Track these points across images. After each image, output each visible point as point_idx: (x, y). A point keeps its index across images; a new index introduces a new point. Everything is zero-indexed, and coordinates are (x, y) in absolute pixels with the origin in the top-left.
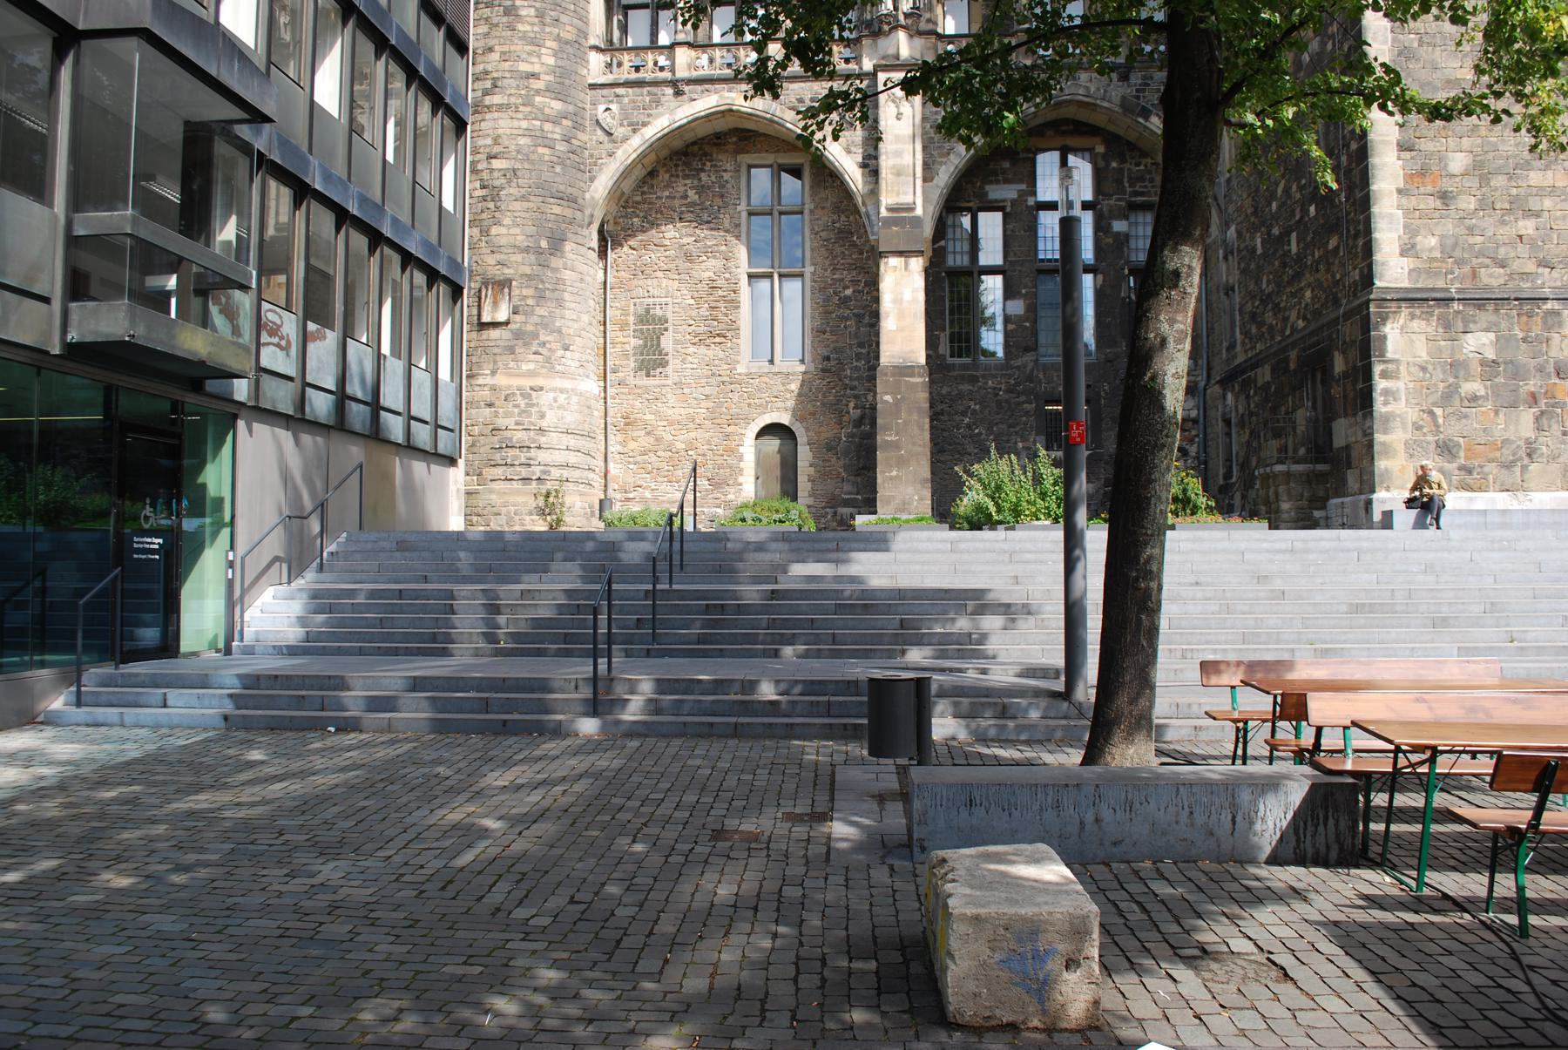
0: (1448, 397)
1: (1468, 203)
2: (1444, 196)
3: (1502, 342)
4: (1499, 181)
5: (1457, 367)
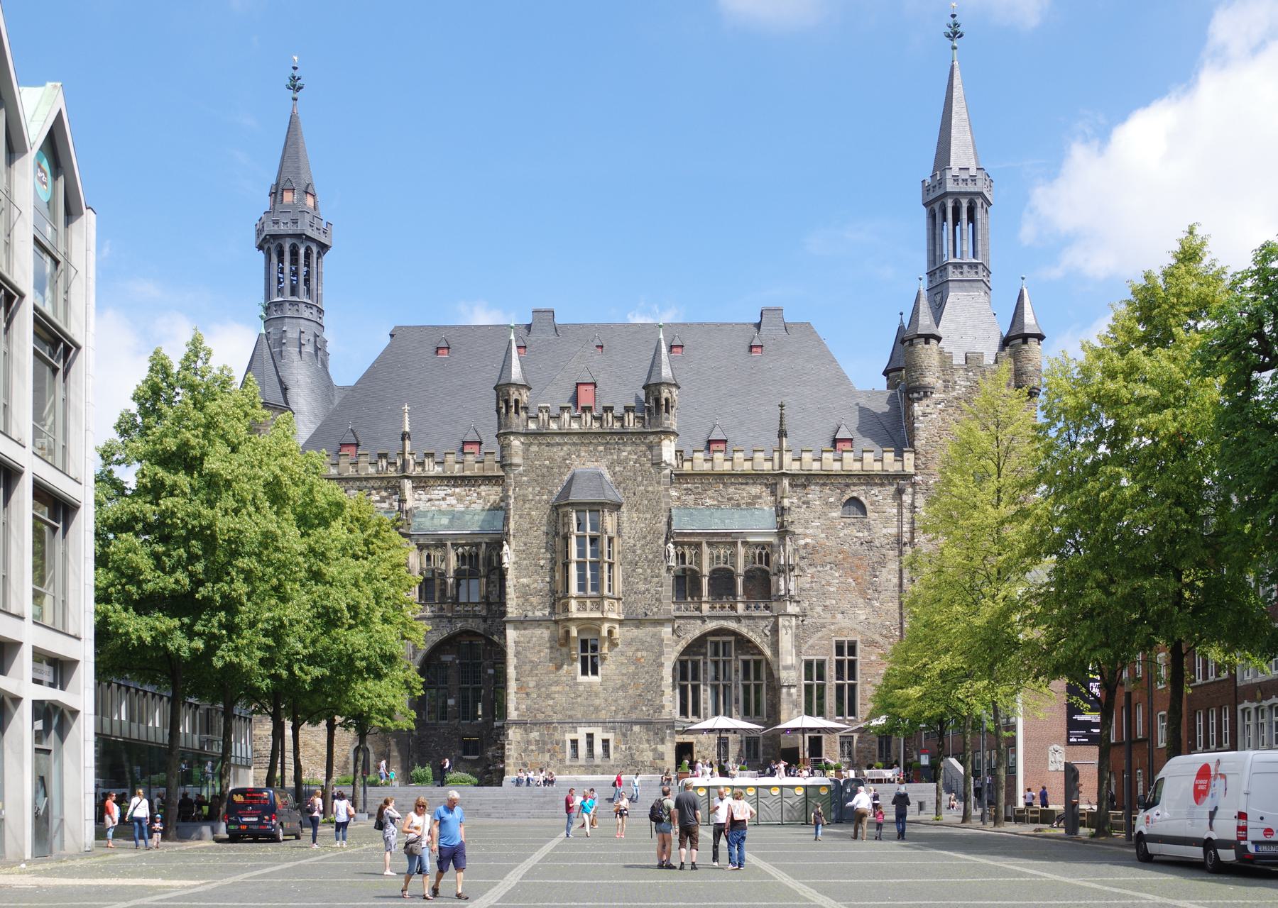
0: (525, 751)
2: (527, 694)
3: (542, 735)
5: (529, 742)
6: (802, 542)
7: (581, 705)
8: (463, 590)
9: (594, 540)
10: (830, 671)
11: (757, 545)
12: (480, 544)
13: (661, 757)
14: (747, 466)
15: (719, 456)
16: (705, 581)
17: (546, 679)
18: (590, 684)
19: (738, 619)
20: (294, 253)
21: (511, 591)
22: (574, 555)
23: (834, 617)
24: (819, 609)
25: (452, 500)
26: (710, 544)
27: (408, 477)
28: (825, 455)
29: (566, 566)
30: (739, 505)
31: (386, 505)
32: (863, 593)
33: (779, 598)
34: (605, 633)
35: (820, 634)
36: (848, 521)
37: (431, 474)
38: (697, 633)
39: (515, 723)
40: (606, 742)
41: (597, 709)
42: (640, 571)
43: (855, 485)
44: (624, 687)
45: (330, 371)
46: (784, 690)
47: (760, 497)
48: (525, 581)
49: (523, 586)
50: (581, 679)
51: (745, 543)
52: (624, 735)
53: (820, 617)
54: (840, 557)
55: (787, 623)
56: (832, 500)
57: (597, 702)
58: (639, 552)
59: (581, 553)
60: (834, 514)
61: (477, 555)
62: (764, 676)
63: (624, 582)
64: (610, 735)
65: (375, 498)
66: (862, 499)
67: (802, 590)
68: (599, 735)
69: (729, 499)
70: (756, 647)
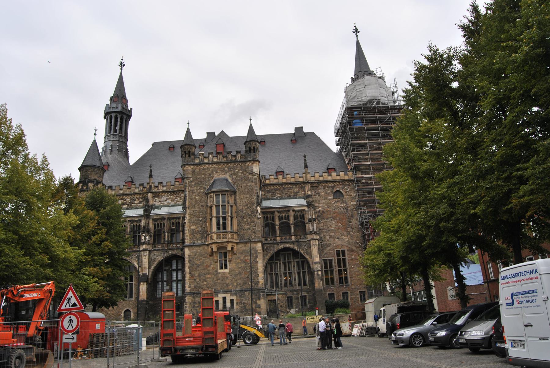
1: (198, 280)
4: (202, 277)
5: (195, 303)
6: (318, 210)
7: (220, 283)
8: (174, 238)
9: (224, 206)
10: (335, 264)
11: (299, 211)
12: (179, 218)
13: (259, 306)
14: (293, 180)
15: (280, 177)
16: (277, 228)
17: (203, 272)
18: (224, 273)
19: (293, 243)
20: (116, 118)
21: (187, 232)
22: (214, 214)
23: (334, 240)
24: (328, 237)
25: (169, 201)
26: (277, 211)
27: (151, 192)
28: (324, 174)
29: (211, 219)
30: (290, 196)
31: (141, 205)
32: (345, 229)
33: (311, 233)
34: (229, 248)
35: (329, 248)
36: (336, 200)
37: (161, 190)
38: (275, 250)
39: (190, 294)
40: (232, 301)
41: (227, 285)
42: (245, 220)
43: (337, 185)
44: (240, 274)
45: (129, 161)
46: (316, 273)
47: (299, 192)
48: (193, 227)
49: (193, 230)
50: (220, 271)
51: (293, 210)
52: (241, 296)
53: (328, 240)
54: (335, 215)
55: (314, 243)
56: (329, 192)
57: (227, 282)
58: (244, 212)
59: (218, 213)
60: (330, 198)
61: (179, 223)
62: (306, 268)
63: (238, 225)
64: (234, 298)
65: (137, 202)
66: (341, 191)
67: (320, 229)
68: (229, 297)
69: (286, 194)
70: (302, 255)
